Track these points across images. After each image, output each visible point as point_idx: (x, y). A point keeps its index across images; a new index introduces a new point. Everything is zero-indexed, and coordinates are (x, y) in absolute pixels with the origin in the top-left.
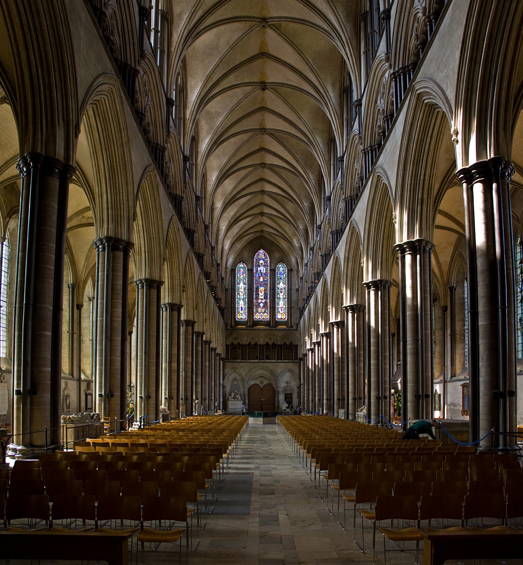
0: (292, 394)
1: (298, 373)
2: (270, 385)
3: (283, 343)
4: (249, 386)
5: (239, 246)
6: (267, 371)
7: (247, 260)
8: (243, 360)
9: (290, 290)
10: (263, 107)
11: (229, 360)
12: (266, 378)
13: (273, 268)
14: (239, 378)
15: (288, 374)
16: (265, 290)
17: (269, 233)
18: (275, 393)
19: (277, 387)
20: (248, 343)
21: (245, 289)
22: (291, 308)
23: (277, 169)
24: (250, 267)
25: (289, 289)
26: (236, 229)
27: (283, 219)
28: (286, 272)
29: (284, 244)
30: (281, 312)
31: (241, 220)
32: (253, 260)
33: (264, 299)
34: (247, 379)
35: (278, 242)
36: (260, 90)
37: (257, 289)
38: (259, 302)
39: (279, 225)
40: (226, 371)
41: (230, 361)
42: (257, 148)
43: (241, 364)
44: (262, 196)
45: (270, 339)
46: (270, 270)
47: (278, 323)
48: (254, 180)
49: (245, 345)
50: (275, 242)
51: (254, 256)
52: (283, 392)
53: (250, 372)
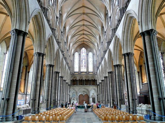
1: (97, 90)
9: (93, 61)
13: (87, 53)
15: (93, 90)
17: (86, 42)
29: (91, 45)
34: (78, 92)
37: (82, 61)
39: (89, 38)
40: (71, 89)
45: (87, 78)
46: (87, 54)
47: (89, 72)
50: (88, 45)
52: (92, 97)
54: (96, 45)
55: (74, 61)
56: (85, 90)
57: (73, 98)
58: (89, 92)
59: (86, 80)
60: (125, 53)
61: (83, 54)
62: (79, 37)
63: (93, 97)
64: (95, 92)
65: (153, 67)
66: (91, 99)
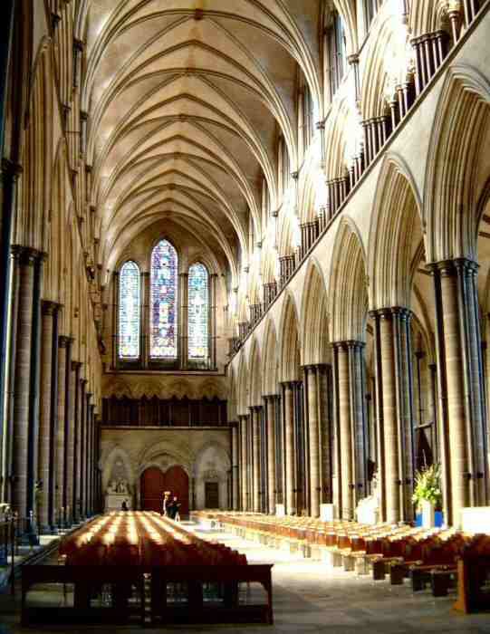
2: (178, 469)
3: (201, 396)
5: (128, 235)
13: (183, 272)
16: (169, 308)
19: (194, 472)
20: (141, 395)
21: (135, 306)
22: (215, 338)
24: (144, 270)
25: (210, 307)
26: (127, 210)
28: (207, 278)
33: (169, 322)
37: (156, 305)
40: (105, 444)
43: (129, 432)
45: (180, 389)
46: (180, 275)
47: (193, 366)
49: (137, 401)
55: (116, 306)
57: (114, 484)
61: (160, 272)
63: (209, 481)
66: (200, 490)
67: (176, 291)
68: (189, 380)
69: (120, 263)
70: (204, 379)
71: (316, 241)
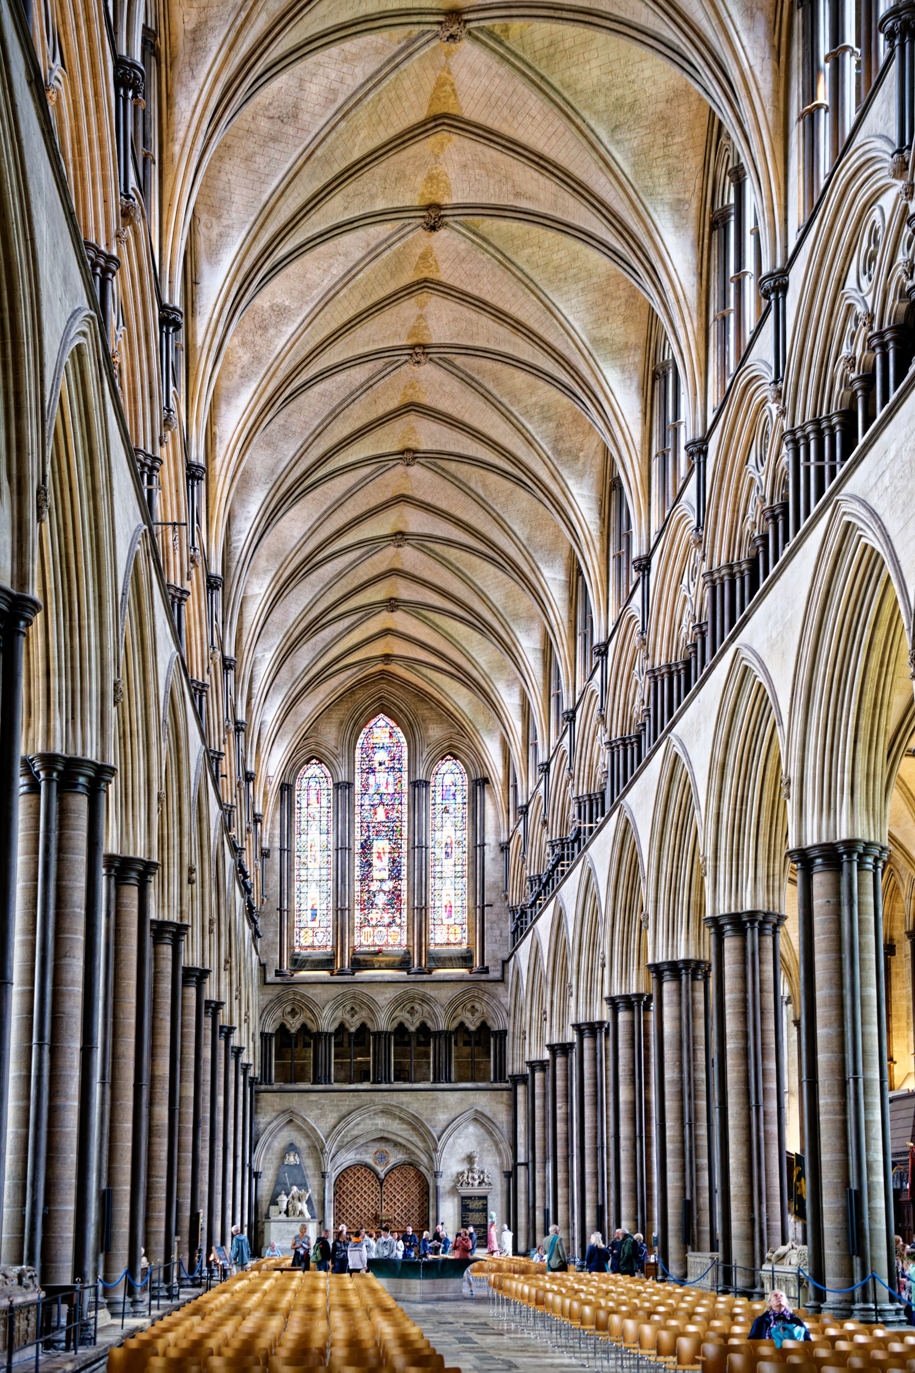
0: (485, 1198)
1: (505, 1128)
3: (455, 1024)
4: (339, 1170)
5: (308, 707)
6: (401, 1118)
7: (333, 754)
8: (319, 1083)
10: (426, 280)
11: (270, 1083)
12: (396, 1144)
13: (421, 775)
14: (302, 1144)
15: (472, 1129)
18: (427, 1193)
19: (436, 1175)
20: (336, 1025)
23: (452, 467)
24: (343, 776)
27: (462, 620)
30: (446, 922)
31: (324, 627)
32: (354, 753)
33: (391, 878)
34: (330, 1147)
35: (441, 690)
36: (420, 230)
37: (366, 847)
38: (373, 888)
40: (262, 1120)
41: (276, 1086)
42: (394, 404)
43: (313, 1097)
44: (395, 549)
45: (412, 1011)
48: (373, 504)
51: (357, 738)
52: (454, 1191)
53: (342, 1124)
54: (510, 702)
56: (396, 1128)
57: (283, 1200)
58: (432, 1151)
59: (401, 1029)
60: (723, 910)
62: (349, 630)
64: (488, 1144)
65: (833, 1052)
67: (405, 818)
68: (430, 991)
69: (293, 767)
70: (459, 989)
71: (793, 541)
